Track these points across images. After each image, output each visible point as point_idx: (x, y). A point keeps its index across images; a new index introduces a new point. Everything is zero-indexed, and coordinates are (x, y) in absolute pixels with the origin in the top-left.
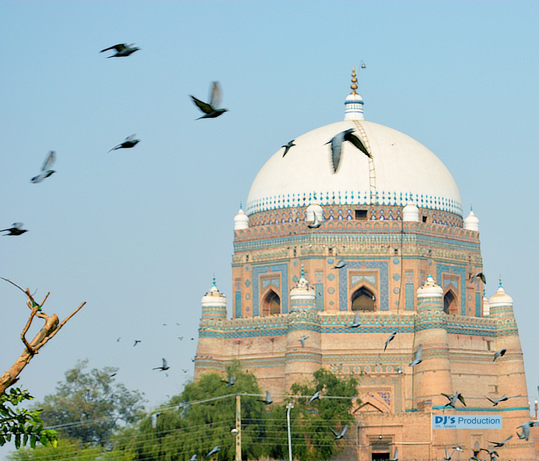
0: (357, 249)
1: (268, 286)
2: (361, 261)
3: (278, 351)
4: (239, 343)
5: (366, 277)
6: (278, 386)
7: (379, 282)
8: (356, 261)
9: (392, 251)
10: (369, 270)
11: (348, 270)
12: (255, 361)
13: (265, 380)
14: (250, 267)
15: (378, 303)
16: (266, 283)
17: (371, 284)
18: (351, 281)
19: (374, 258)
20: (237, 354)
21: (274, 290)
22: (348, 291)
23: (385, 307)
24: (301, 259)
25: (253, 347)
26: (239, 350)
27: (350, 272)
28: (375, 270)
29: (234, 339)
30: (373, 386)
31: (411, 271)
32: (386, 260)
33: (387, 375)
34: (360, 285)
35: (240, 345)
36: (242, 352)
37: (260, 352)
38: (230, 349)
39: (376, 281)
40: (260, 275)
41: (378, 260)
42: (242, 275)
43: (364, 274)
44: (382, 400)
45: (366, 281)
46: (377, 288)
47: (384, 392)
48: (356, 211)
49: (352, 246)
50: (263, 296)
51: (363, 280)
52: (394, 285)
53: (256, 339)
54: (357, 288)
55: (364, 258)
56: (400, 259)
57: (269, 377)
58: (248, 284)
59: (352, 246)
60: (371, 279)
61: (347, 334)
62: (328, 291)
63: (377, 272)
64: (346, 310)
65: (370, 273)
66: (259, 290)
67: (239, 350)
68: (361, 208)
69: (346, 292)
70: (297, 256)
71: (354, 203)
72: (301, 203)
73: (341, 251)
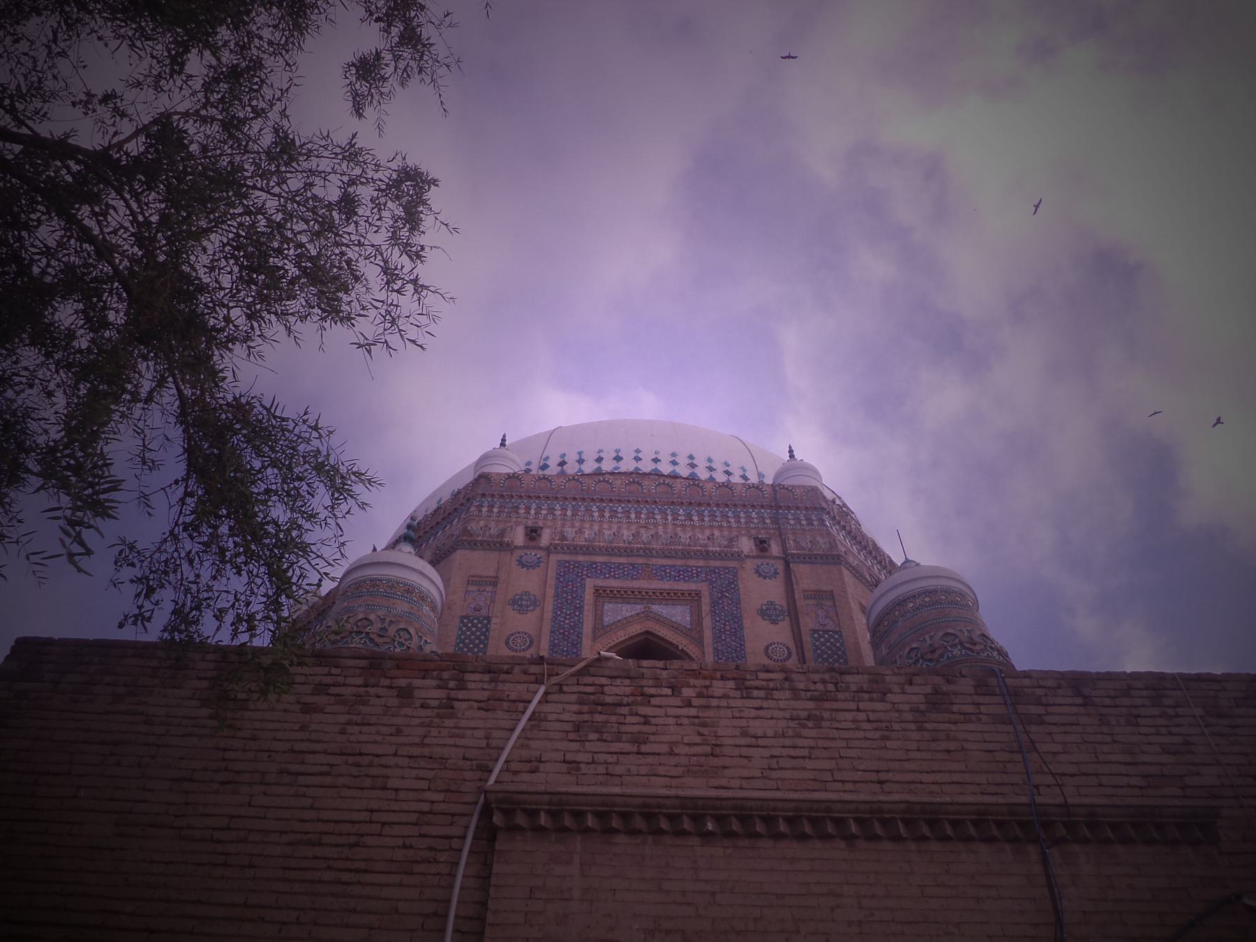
2: (641, 561)
5: (655, 608)
8: (623, 560)
11: (590, 584)
17: (675, 627)
18: (598, 616)
19: (686, 555)
28: (692, 586)
32: (731, 564)
34: (636, 629)
41: (701, 563)
46: (700, 642)
51: (648, 615)
55: (648, 552)
56: (780, 566)
60: (679, 614)
62: (507, 643)
63: (698, 594)
65: (670, 597)
71: (622, 470)
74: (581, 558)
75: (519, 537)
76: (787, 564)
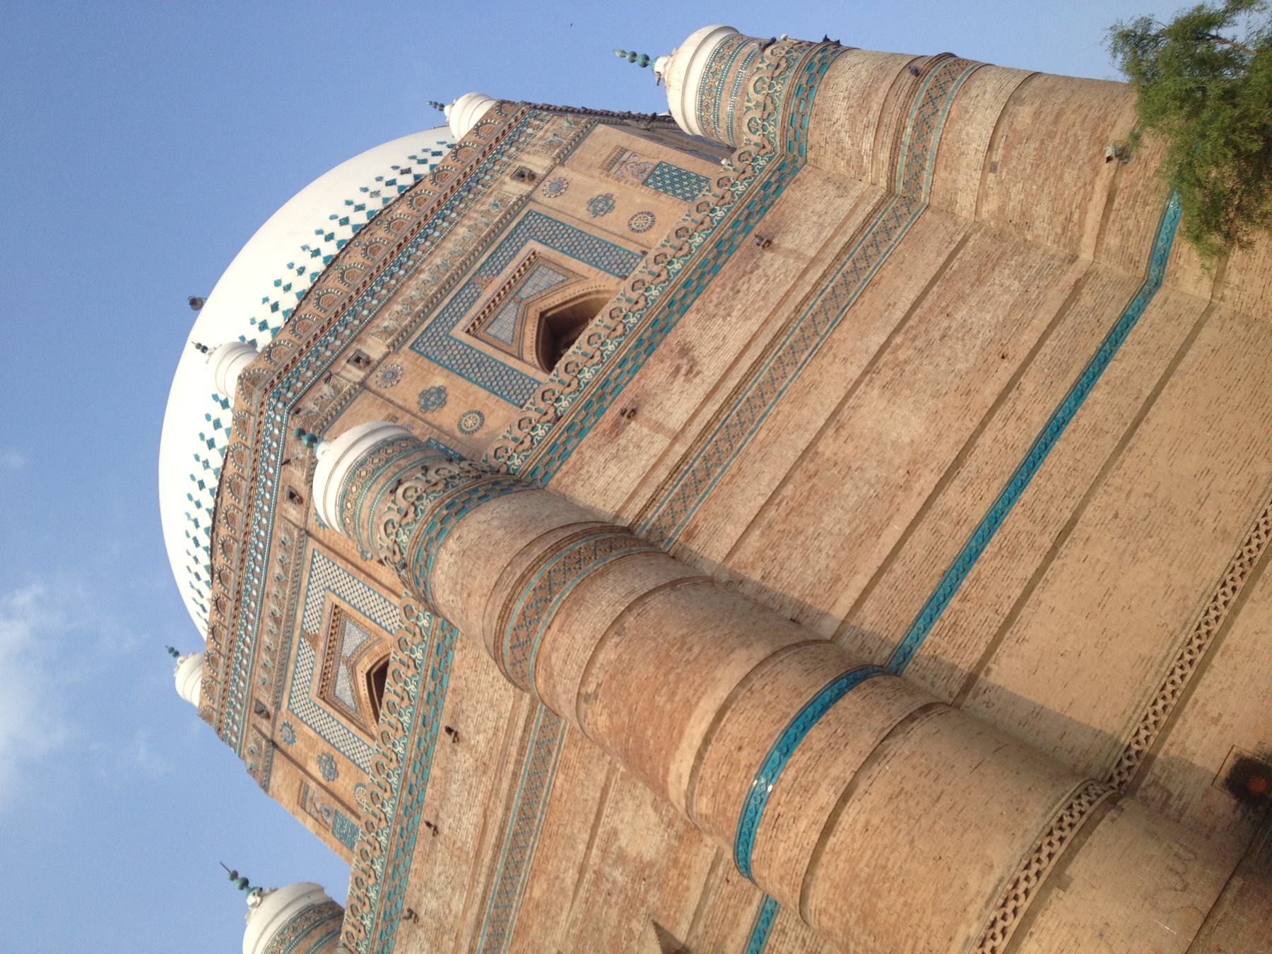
1: (522, 321)
3: (828, 233)
4: (631, 413)
6: (980, 281)
12: (770, 362)
13: (898, 339)
16: (503, 327)
25: (702, 351)
26: (658, 427)
35: (645, 412)
36: (676, 420)
40: (458, 332)
53: (690, 327)
57: (898, 315)
66: (500, 357)
67: (658, 427)
70: (539, 171)
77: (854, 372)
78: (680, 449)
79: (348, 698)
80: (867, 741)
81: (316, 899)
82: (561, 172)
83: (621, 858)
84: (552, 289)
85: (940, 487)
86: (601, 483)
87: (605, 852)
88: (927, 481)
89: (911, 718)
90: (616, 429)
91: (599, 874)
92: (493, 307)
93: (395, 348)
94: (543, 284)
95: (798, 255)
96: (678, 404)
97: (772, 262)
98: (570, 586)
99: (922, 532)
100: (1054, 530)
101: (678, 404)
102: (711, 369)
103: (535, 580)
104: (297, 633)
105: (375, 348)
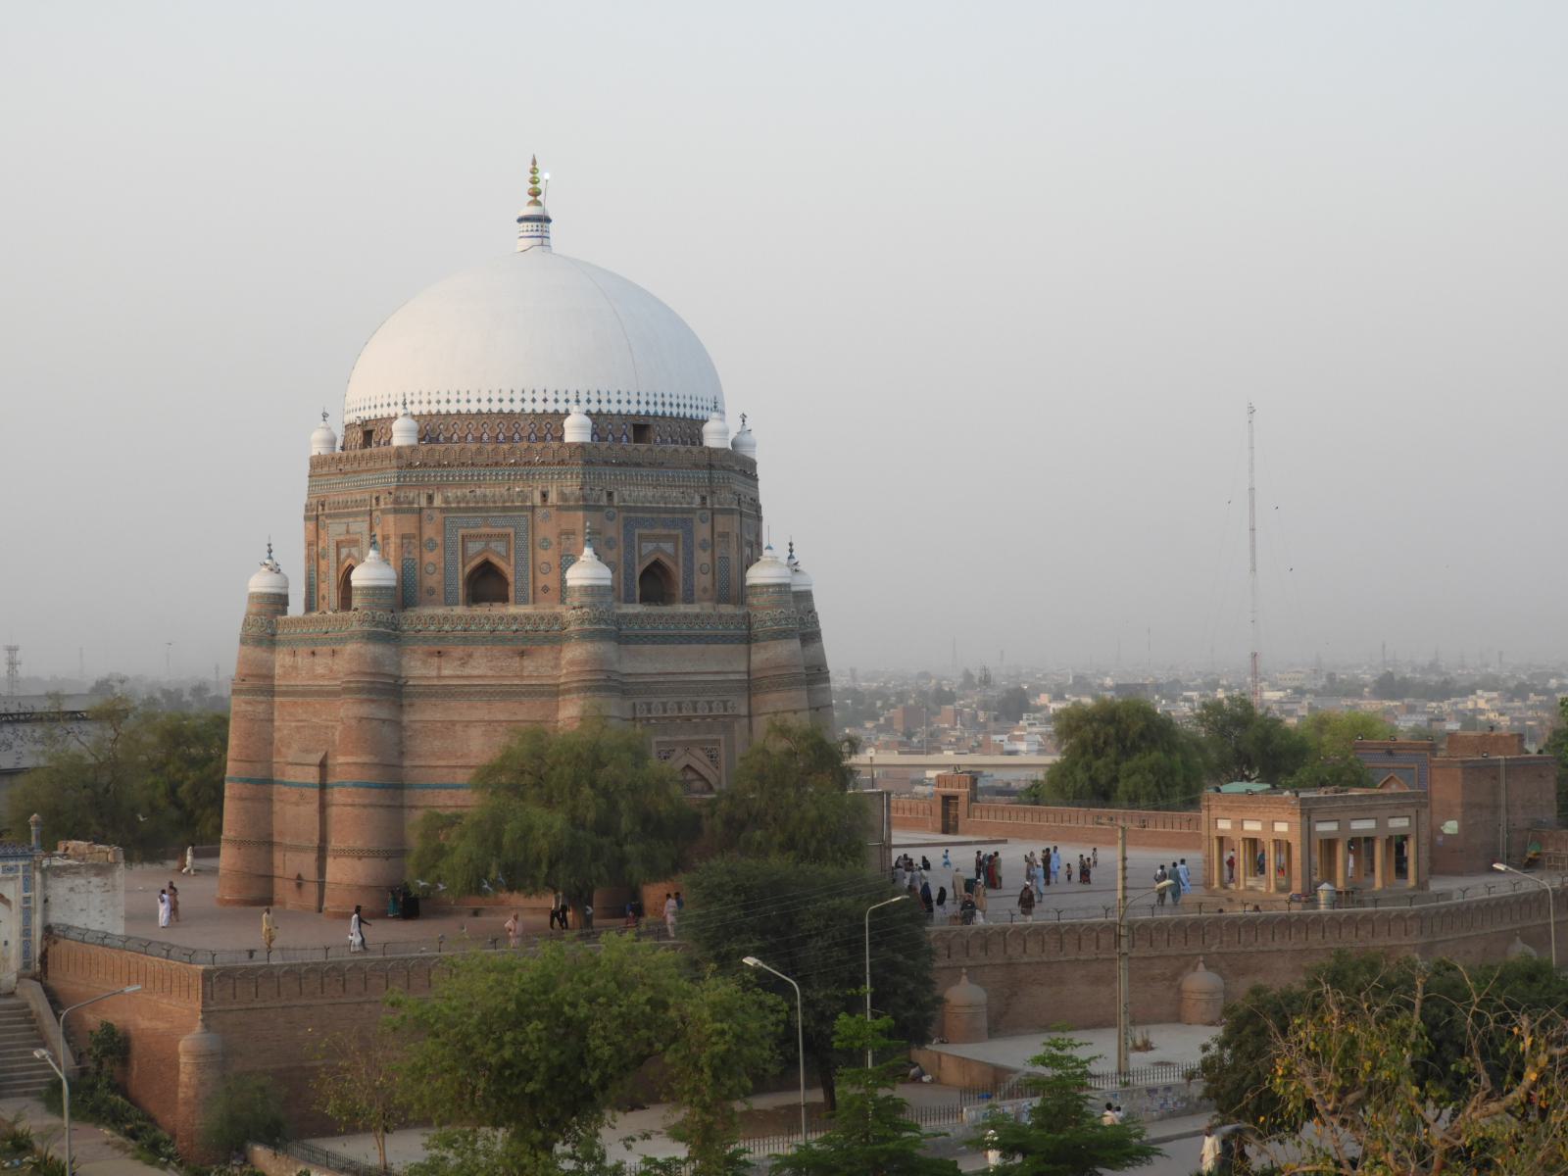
0: (650, 494)
1: (479, 554)
5: (661, 544)
7: (681, 553)
8: (648, 515)
9: (698, 499)
10: (665, 532)
11: (637, 531)
12: (478, 688)
14: (438, 516)
15: (680, 591)
19: (673, 511)
20: (434, 673)
21: (495, 560)
22: (637, 567)
23: (689, 599)
24: (559, 508)
26: (439, 668)
27: (640, 536)
29: (426, 647)
30: (696, 737)
31: (725, 535)
32: (690, 516)
33: (715, 718)
36: (446, 672)
37: (490, 673)
38: (419, 663)
39: (676, 550)
40: (461, 532)
42: (420, 528)
43: (658, 538)
44: (707, 760)
45: (662, 551)
46: (676, 564)
47: (709, 747)
48: (634, 426)
49: (638, 492)
50: (468, 569)
51: (658, 549)
52: (702, 558)
53: (479, 651)
54: (647, 563)
55: (658, 510)
57: (514, 718)
58: (432, 545)
59: (638, 492)
60: (668, 547)
61: (656, 646)
63: (677, 536)
64: (634, 602)
65: (667, 538)
68: (642, 422)
69: (633, 570)
72: (551, 407)
73: (627, 498)
74: (632, 515)
75: (604, 501)
76: (713, 514)
77: (486, 718)
78: (435, 682)
79: (342, 557)
80: (367, 801)
81: (282, 591)
82: (553, 511)
83: (333, 735)
84: (498, 554)
85: (461, 767)
86: (412, 664)
87: (333, 727)
88: (461, 762)
89: (381, 806)
90: (431, 654)
91: (327, 727)
92: (479, 537)
93: (442, 510)
94: (499, 549)
95: (523, 668)
96: (450, 670)
97: (516, 662)
98: (365, 696)
99: (445, 771)
100: (463, 804)
101: (450, 670)
102: (468, 671)
103: (360, 685)
104: (345, 520)
105: (438, 502)
